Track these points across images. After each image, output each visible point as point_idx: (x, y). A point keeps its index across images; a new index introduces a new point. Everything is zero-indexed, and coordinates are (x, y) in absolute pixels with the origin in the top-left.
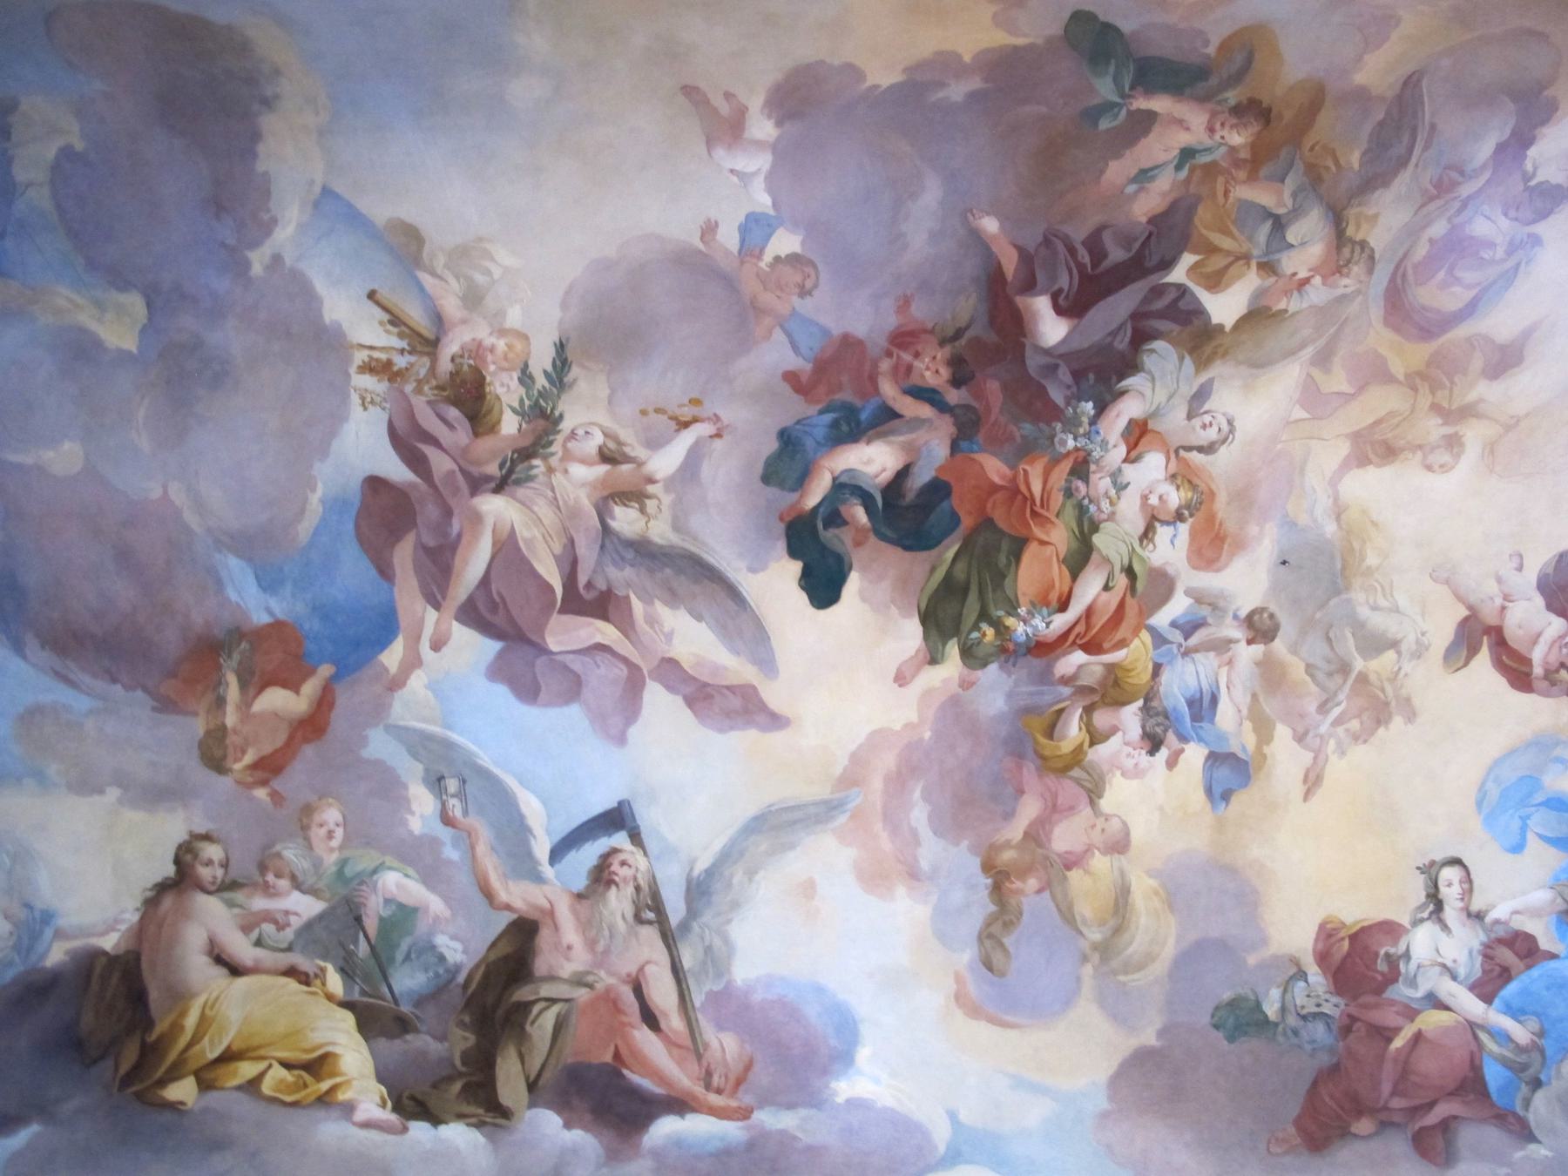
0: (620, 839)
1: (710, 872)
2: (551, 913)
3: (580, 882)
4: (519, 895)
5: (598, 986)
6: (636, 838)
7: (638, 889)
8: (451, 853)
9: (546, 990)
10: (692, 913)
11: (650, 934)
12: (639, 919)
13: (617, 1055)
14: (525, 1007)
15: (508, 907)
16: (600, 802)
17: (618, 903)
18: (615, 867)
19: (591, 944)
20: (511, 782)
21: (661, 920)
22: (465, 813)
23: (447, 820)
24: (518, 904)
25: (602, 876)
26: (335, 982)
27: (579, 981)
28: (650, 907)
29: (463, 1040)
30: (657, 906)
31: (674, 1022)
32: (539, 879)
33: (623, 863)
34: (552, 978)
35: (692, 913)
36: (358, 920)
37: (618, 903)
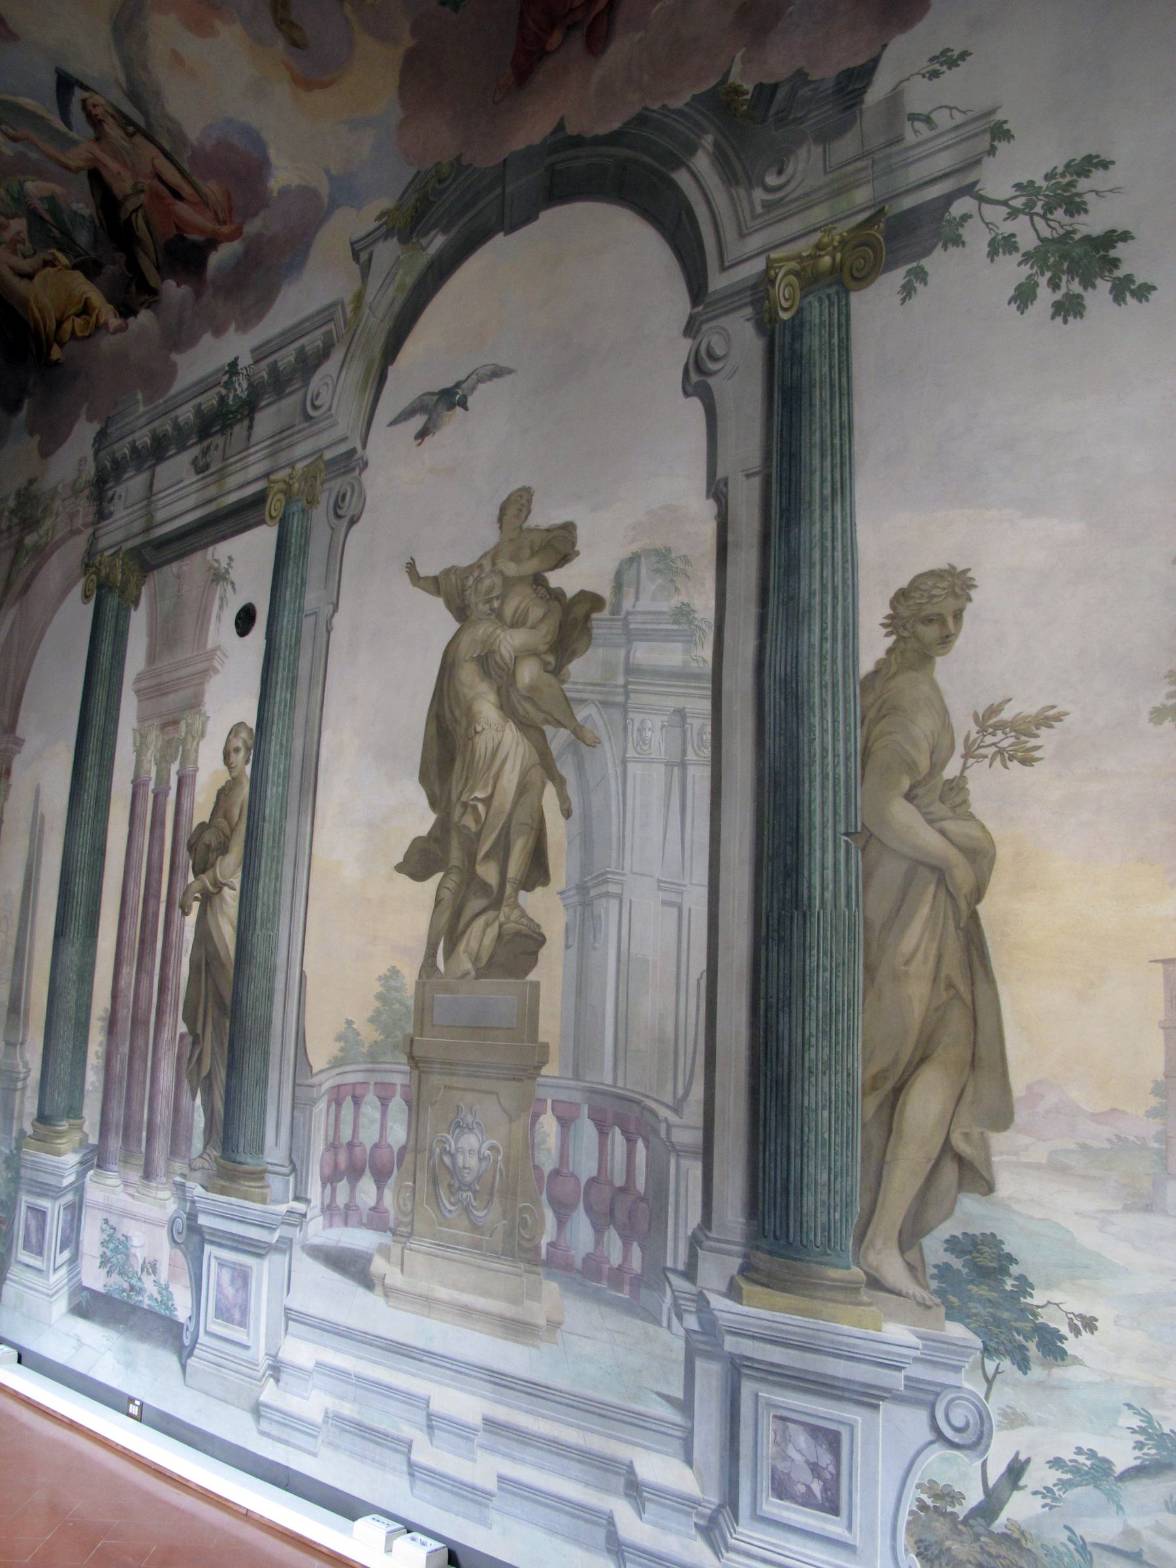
0: (78, 94)
1: (130, 80)
2: (96, 159)
3: (90, 132)
4: (76, 158)
5: (145, 188)
6: (86, 88)
7: (112, 116)
8: (34, 155)
9: (130, 205)
10: (145, 114)
11: (138, 139)
12: (131, 135)
13: (177, 227)
14: (128, 221)
15: (77, 170)
16: (51, 80)
17: (113, 130)
18: (94, 112)
19: (125, 165)
20: (10, 98)
21: (138, 130)
22: (15, 129)
23: (15, 139)
24: (82, 164)
25: (95, 122)
26: (63, 259)
27: (138, 192)
28: (125, 121)
29: (121, 257)
30: (129, 122)
31: (186, 190)
32: (75, 143)
33: (95, 106)
34: (127, 197)
35: (145, 114)
36: (41, 217)
37: (113, 130)
